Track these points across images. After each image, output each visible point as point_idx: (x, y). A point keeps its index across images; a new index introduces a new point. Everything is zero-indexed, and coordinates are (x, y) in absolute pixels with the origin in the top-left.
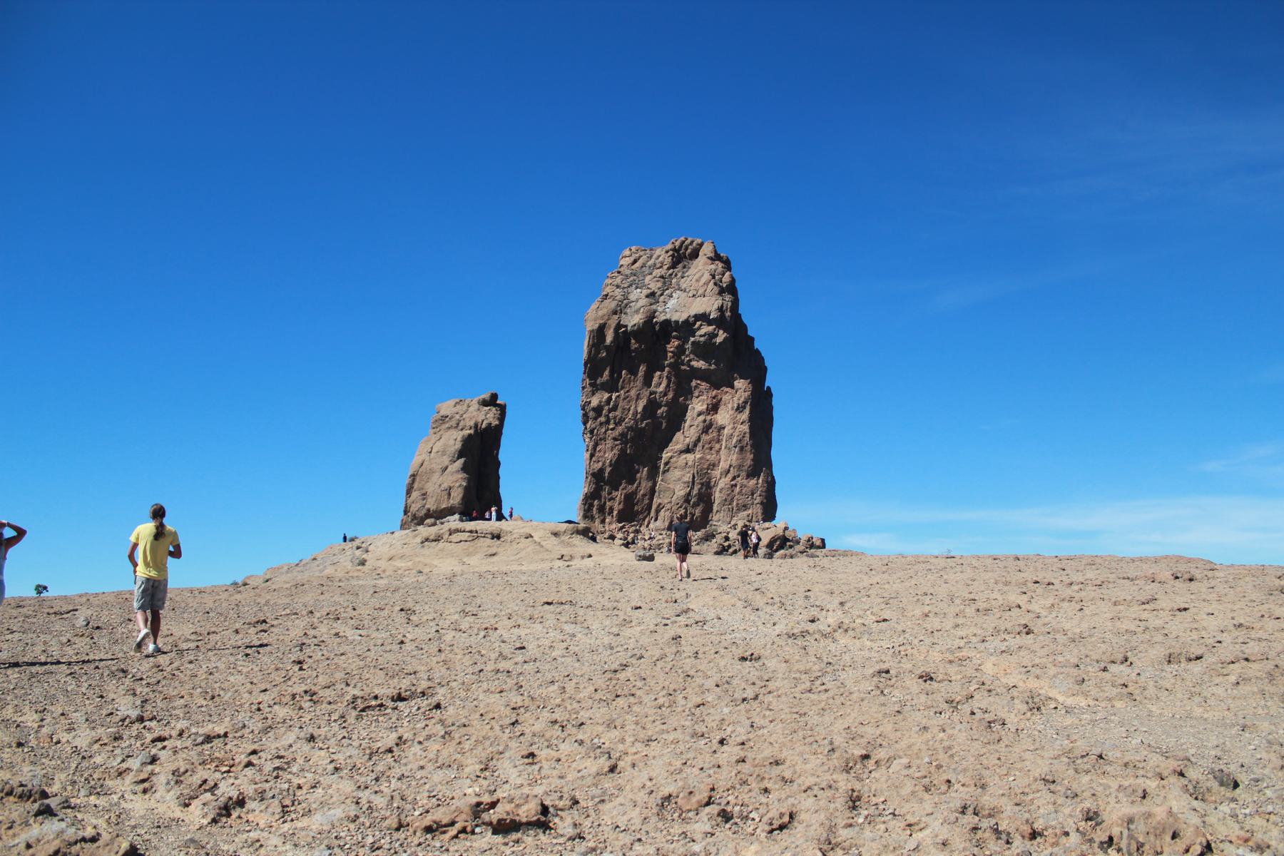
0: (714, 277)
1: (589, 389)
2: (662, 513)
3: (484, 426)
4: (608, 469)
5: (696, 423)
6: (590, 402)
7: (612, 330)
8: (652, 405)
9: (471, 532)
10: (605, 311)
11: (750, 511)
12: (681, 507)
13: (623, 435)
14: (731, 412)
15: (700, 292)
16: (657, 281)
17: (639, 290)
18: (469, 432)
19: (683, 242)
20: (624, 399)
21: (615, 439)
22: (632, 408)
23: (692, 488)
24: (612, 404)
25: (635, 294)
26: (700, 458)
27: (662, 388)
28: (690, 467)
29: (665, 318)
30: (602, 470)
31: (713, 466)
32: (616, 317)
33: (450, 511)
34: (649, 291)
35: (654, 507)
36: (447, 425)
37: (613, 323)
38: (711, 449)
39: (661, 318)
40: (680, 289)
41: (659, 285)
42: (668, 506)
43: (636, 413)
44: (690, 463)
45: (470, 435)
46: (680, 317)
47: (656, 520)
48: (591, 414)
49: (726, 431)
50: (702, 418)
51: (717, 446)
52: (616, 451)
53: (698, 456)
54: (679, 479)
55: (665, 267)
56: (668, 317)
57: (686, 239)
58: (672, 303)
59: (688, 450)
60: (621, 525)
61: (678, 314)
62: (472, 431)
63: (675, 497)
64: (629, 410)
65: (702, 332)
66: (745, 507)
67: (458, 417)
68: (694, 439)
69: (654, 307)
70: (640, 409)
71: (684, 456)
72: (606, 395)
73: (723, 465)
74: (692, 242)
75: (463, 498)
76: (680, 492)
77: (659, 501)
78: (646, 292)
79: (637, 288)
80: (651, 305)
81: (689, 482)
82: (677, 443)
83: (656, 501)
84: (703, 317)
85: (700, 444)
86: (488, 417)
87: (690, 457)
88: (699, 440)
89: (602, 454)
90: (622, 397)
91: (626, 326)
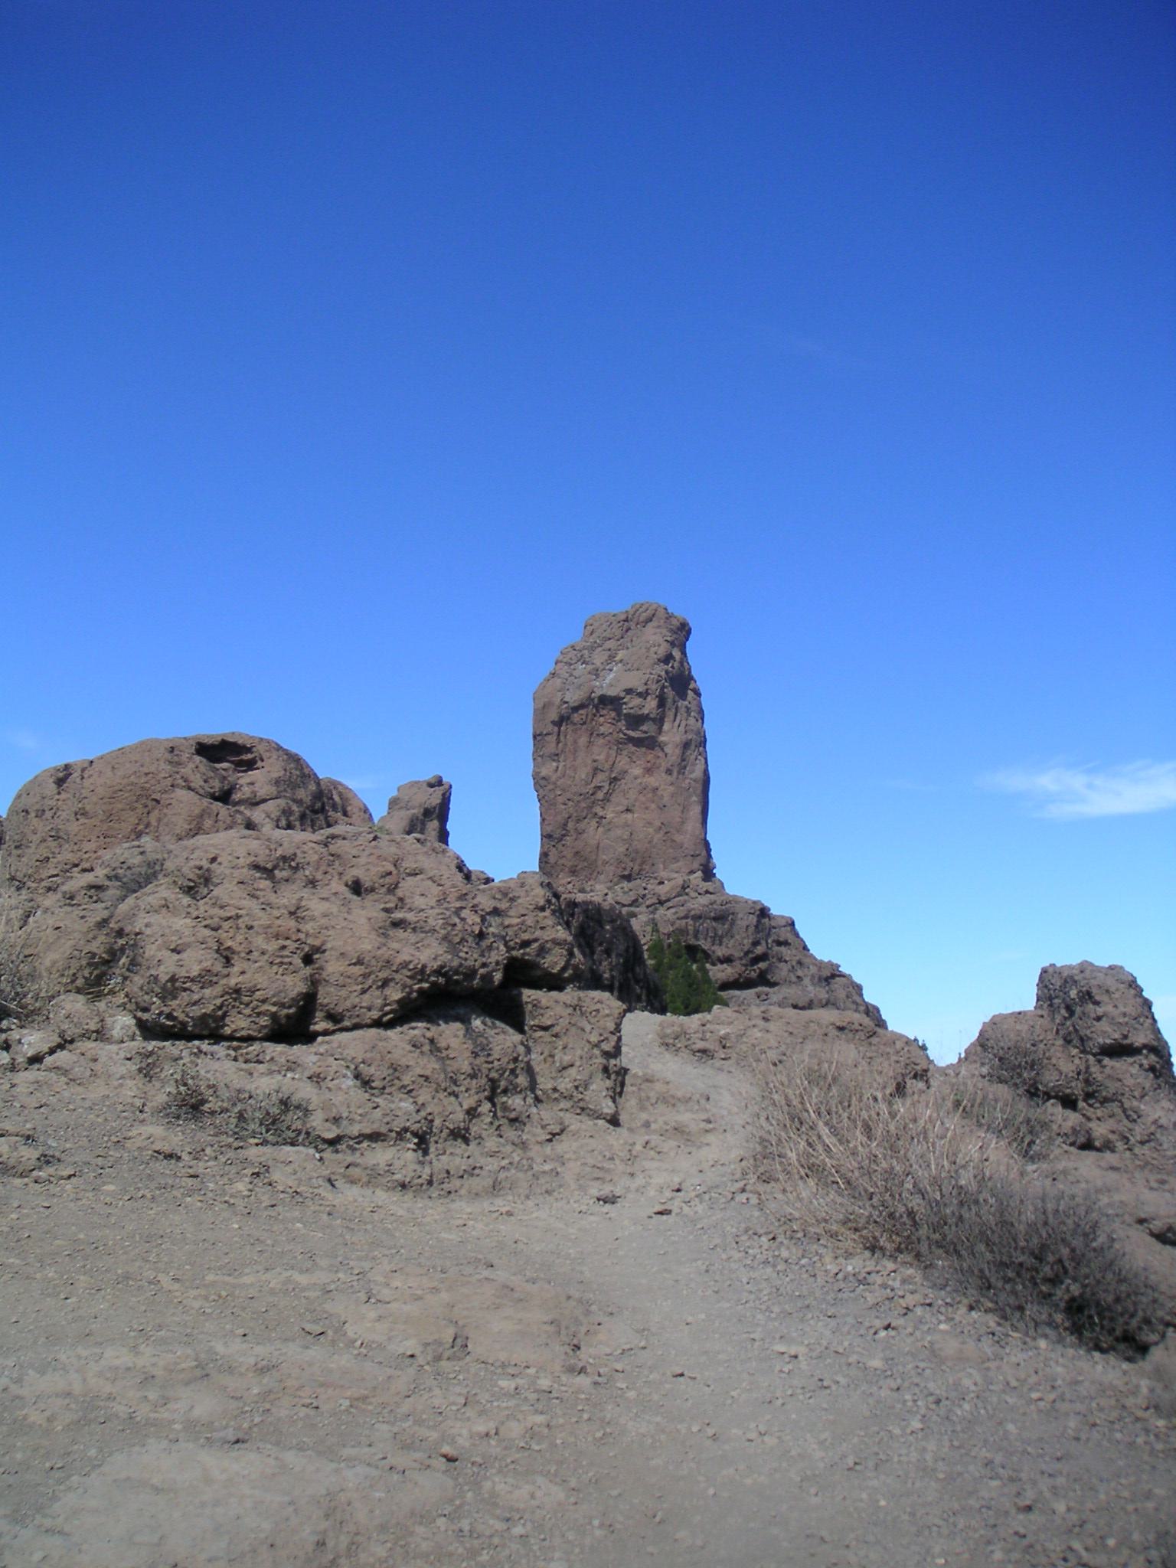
1: (539, 759)
14: (663, 774)
27: (602, 757)
37: (557, 701)
38: (647, 808)
39: (598, 693)
46: (612, 692)
48: (543, 782)
49: (659, 793)
50: (639, 781)
51: (653, 806)
65: (630, 705)
66: (676, 859)
70: (583, 777)
71: (624, 816)
72: (554, 764)
77: (604, 857)
78: (590, 667)
84: (629, 691)
87: (629, 816)
91: (566, 702)
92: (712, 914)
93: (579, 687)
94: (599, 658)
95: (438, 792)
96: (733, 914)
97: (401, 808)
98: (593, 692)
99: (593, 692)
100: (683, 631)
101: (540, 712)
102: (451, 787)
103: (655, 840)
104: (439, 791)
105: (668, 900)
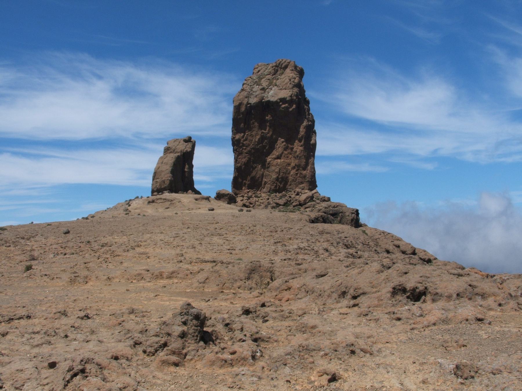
0: (290, 80)
2: (267, 185)
3: (184, 151)
4: (243, 166)
5: (281, 146)
6: (235, 137)
7: (244, 105)
8: (263, 138)
9: (164, 199)
10: (242, 97)
11: (304, 185)
12: (274, 183)
13: (250, 151)
15: (284, 87)
16: (267, 82)
17: (258, 86)
18: (178, 154)
19: (281, 62)
20: (250, 136)
21: (246, 153)
22: (253, 140)
23: (279, 175)
24: (244, 138)
25: (256, 88)
26: (283, 161)
28: (279, 165)
29: (267, 100)
30: (240, 167)
31: (289, 164)
32: (246, 99)
33: (165, 189)
34: (262, 87)
35: (263, 183)
36: (170, 151)
40: (276, 85)
41: (267, 83)
42: (269, 182)
43: (255, 141)
44: (279, 164)
45: (178, 156)
47: (264, 188)
51: (291, 156)
52: (246, 159)
53: (282, 160)
54: (274, 171)
55: (271, 74)
56: (269, 99)
57: (282, 60)
58: (272, 92)
59: (279, 157)
60: (248, 190)
61: (273, 98)
62: (179, 154)
63: (272, 179)
64: (252, 140)
66: (302, 183)
67: (174, 147)
68: (280, 153)
69: (263, 95)
70: (257, 140)
73: (293, 164)
74: (285, 62)
75: (169, 184)
76: (274, 176)
77: (266, 180)
78: (261, 87)
79: (257, 85)
80: (262, 93)
81: (277, 172)
82: (273, 155)
83: (264, 180)
85: (283, 155)
86: (186, 147)
87: (279, 161)
88: (283, 153)
89: (240, 160)
90: (249, 134)
91: (251, 104)
92: (331, 212)
93: (256, 96)
94: (264, 83)
95: (190, 145)
96: (341, 212)
97: (171, 152)
98: (263, 99)
99: (263, 99)
100: (301, 73)
101: (237, 109)
102: (195, 142)
103: (292, 173)
104: (190, 145)
105: (305, 204)
